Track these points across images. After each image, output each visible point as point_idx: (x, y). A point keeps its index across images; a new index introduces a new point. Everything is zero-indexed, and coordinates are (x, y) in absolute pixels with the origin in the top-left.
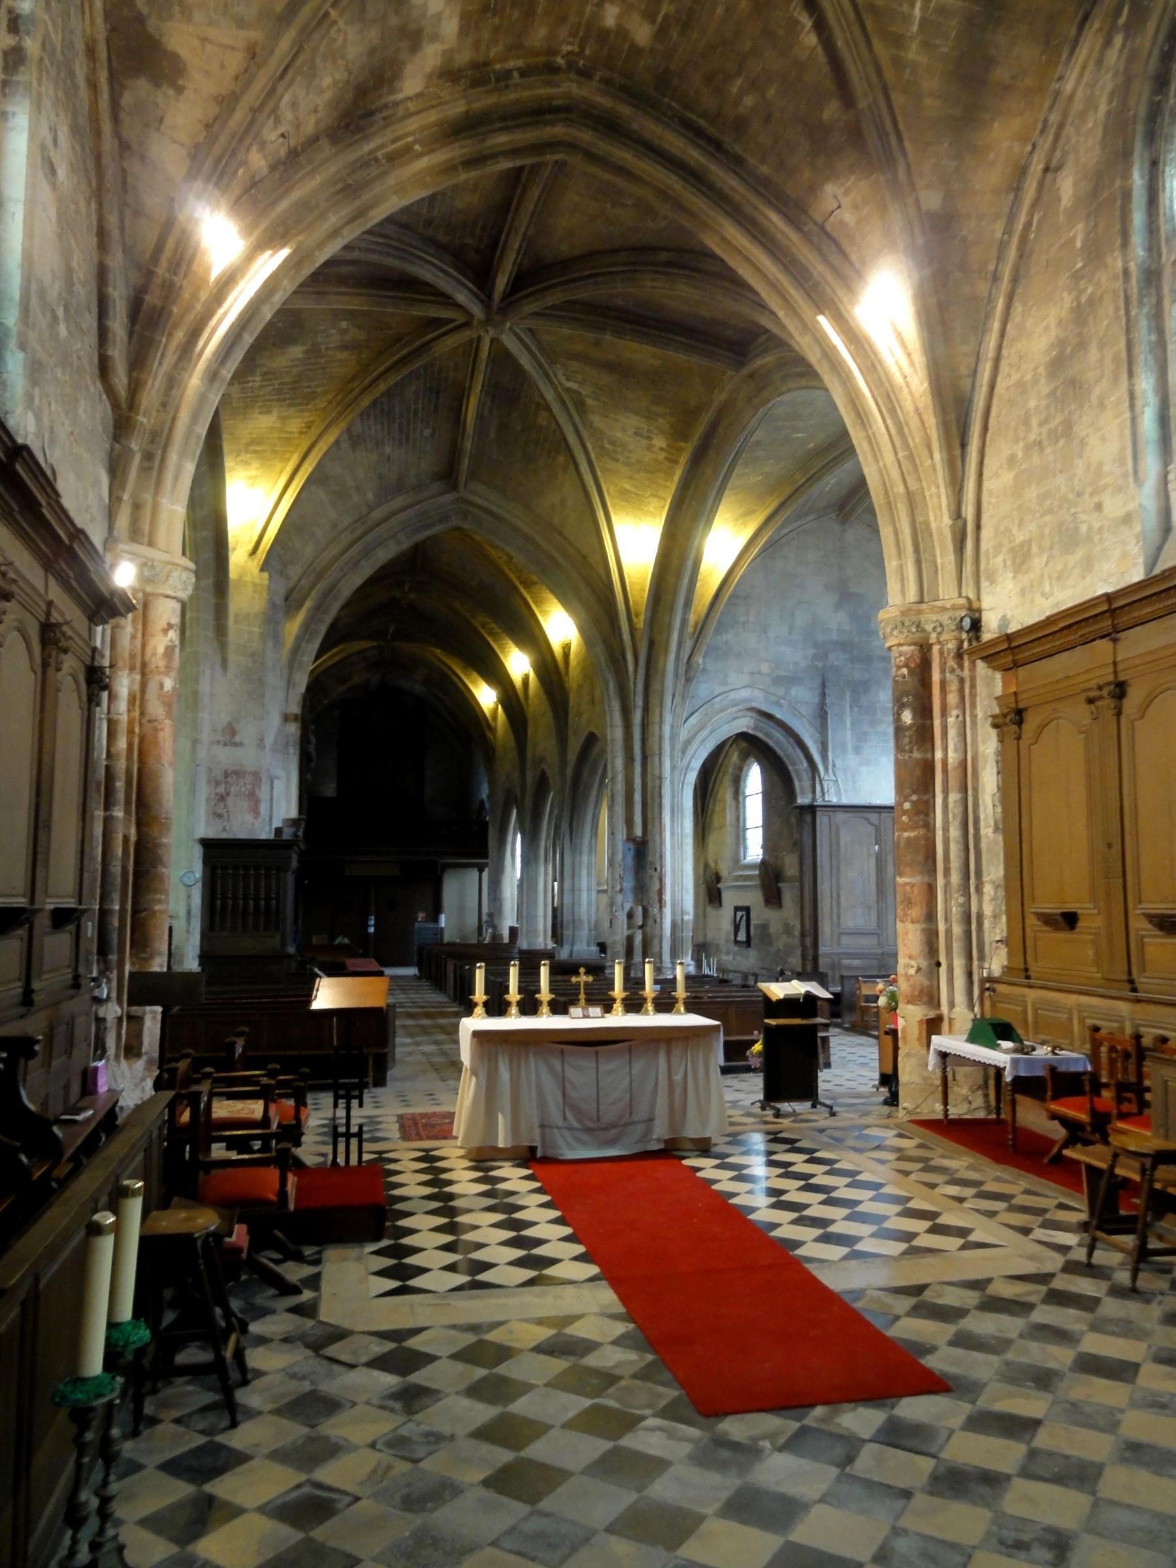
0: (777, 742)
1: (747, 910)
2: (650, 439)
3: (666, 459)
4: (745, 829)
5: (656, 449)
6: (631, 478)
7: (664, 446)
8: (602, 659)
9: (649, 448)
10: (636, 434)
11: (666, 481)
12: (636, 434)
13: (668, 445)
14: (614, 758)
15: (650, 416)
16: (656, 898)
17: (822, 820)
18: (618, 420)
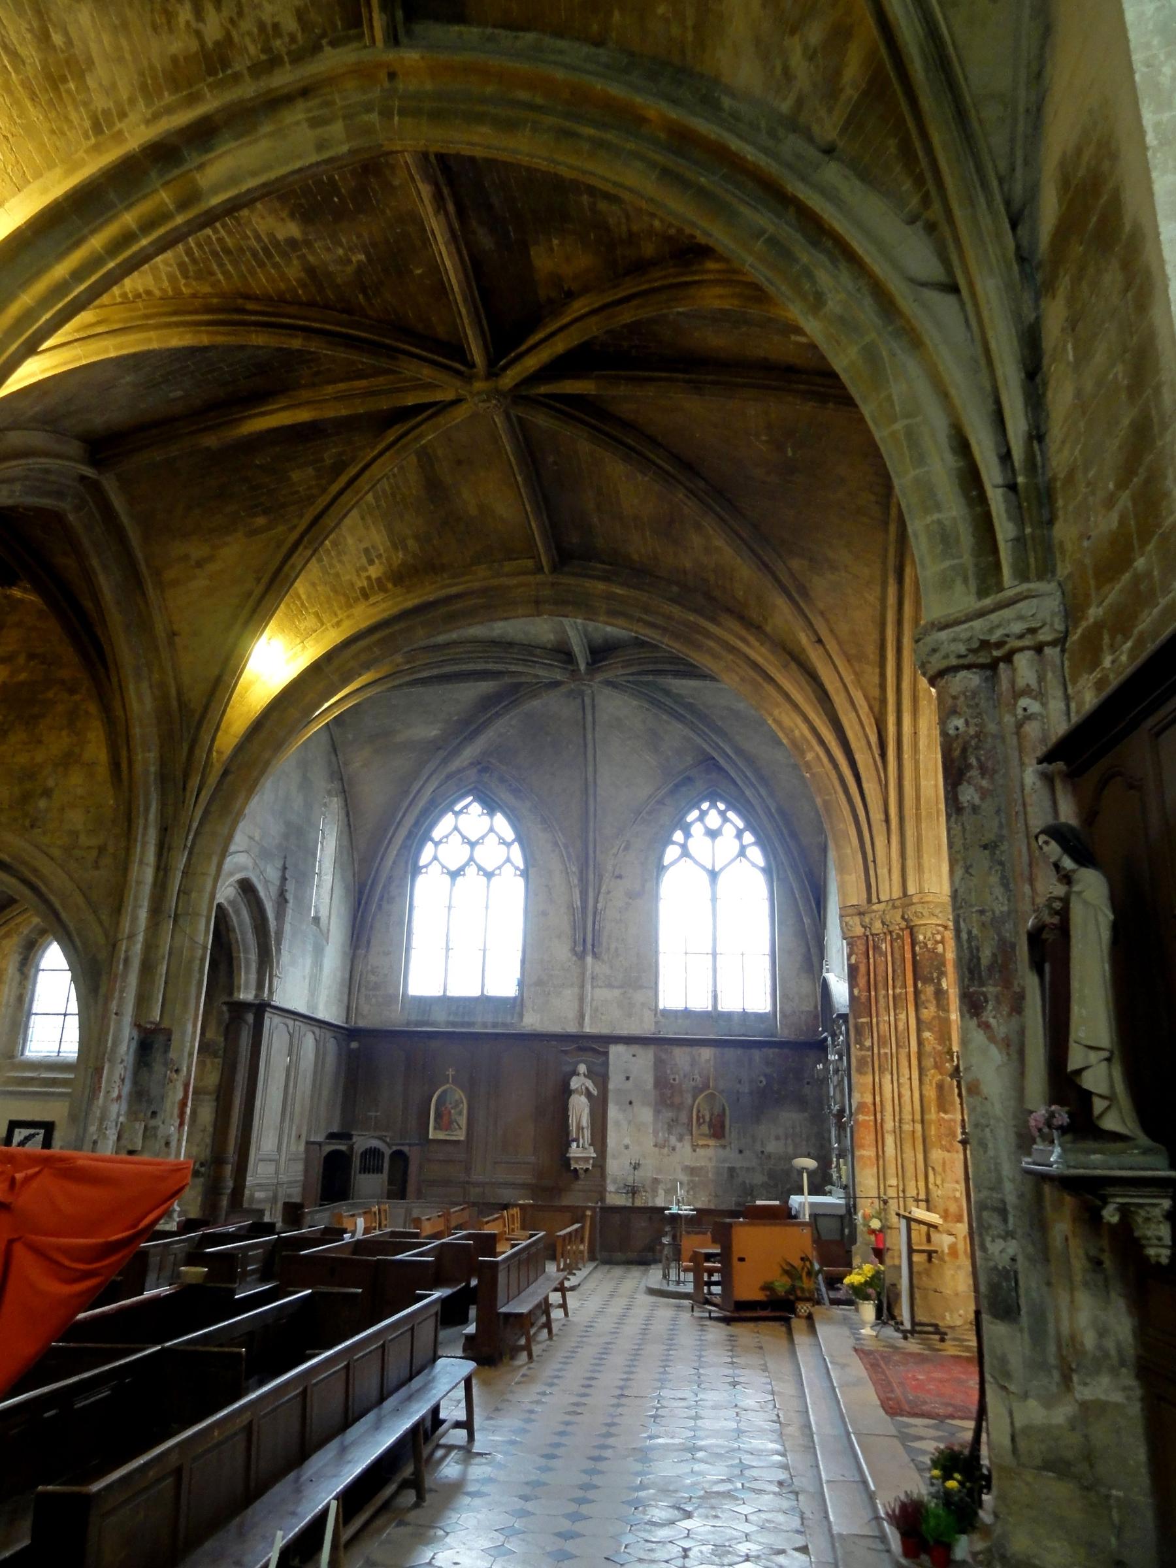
0: (241, 923)
1: (49, 1128)
2: (371, 562)
3: (362, 589)
4: (29, 1014)
5: (364, 575)
6: (314, 585)
7: (374, 576)
8: (152, 769)
9: (360, 570)
10: (366, 551)
11: (341, 608)
12: (366, 551)
13: (379, 580)
14: (136, 907)
15: (397, 543)
16: (176, 1112)
17: (271, 1021)
18: (367, 528)
